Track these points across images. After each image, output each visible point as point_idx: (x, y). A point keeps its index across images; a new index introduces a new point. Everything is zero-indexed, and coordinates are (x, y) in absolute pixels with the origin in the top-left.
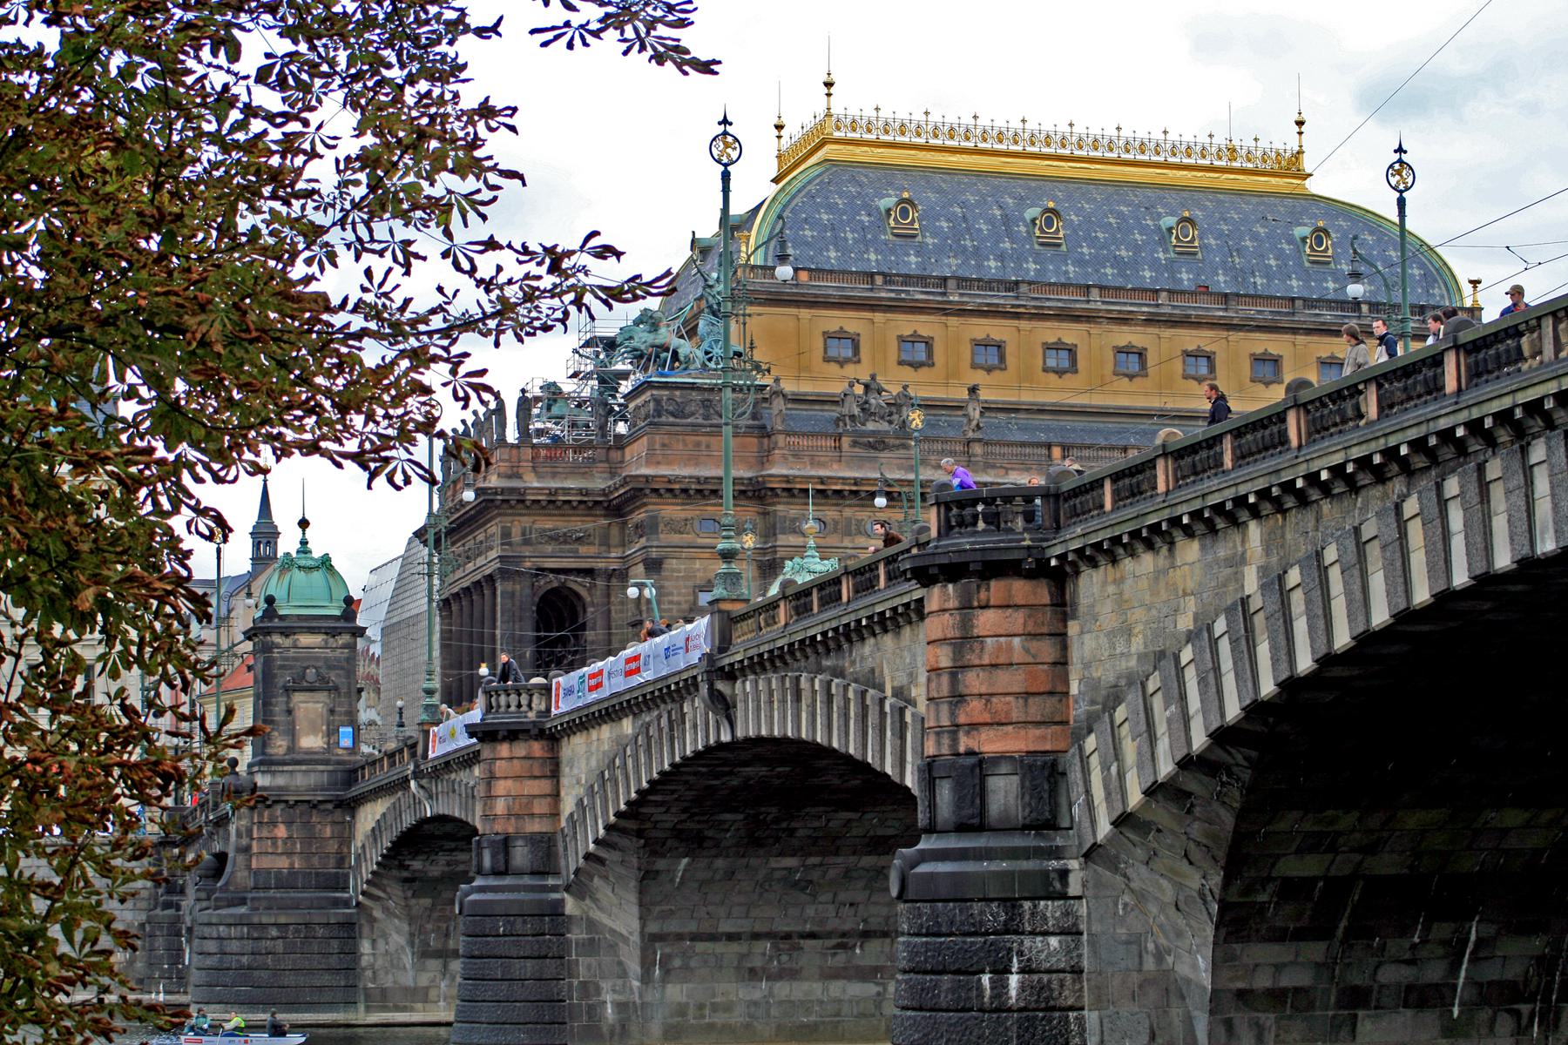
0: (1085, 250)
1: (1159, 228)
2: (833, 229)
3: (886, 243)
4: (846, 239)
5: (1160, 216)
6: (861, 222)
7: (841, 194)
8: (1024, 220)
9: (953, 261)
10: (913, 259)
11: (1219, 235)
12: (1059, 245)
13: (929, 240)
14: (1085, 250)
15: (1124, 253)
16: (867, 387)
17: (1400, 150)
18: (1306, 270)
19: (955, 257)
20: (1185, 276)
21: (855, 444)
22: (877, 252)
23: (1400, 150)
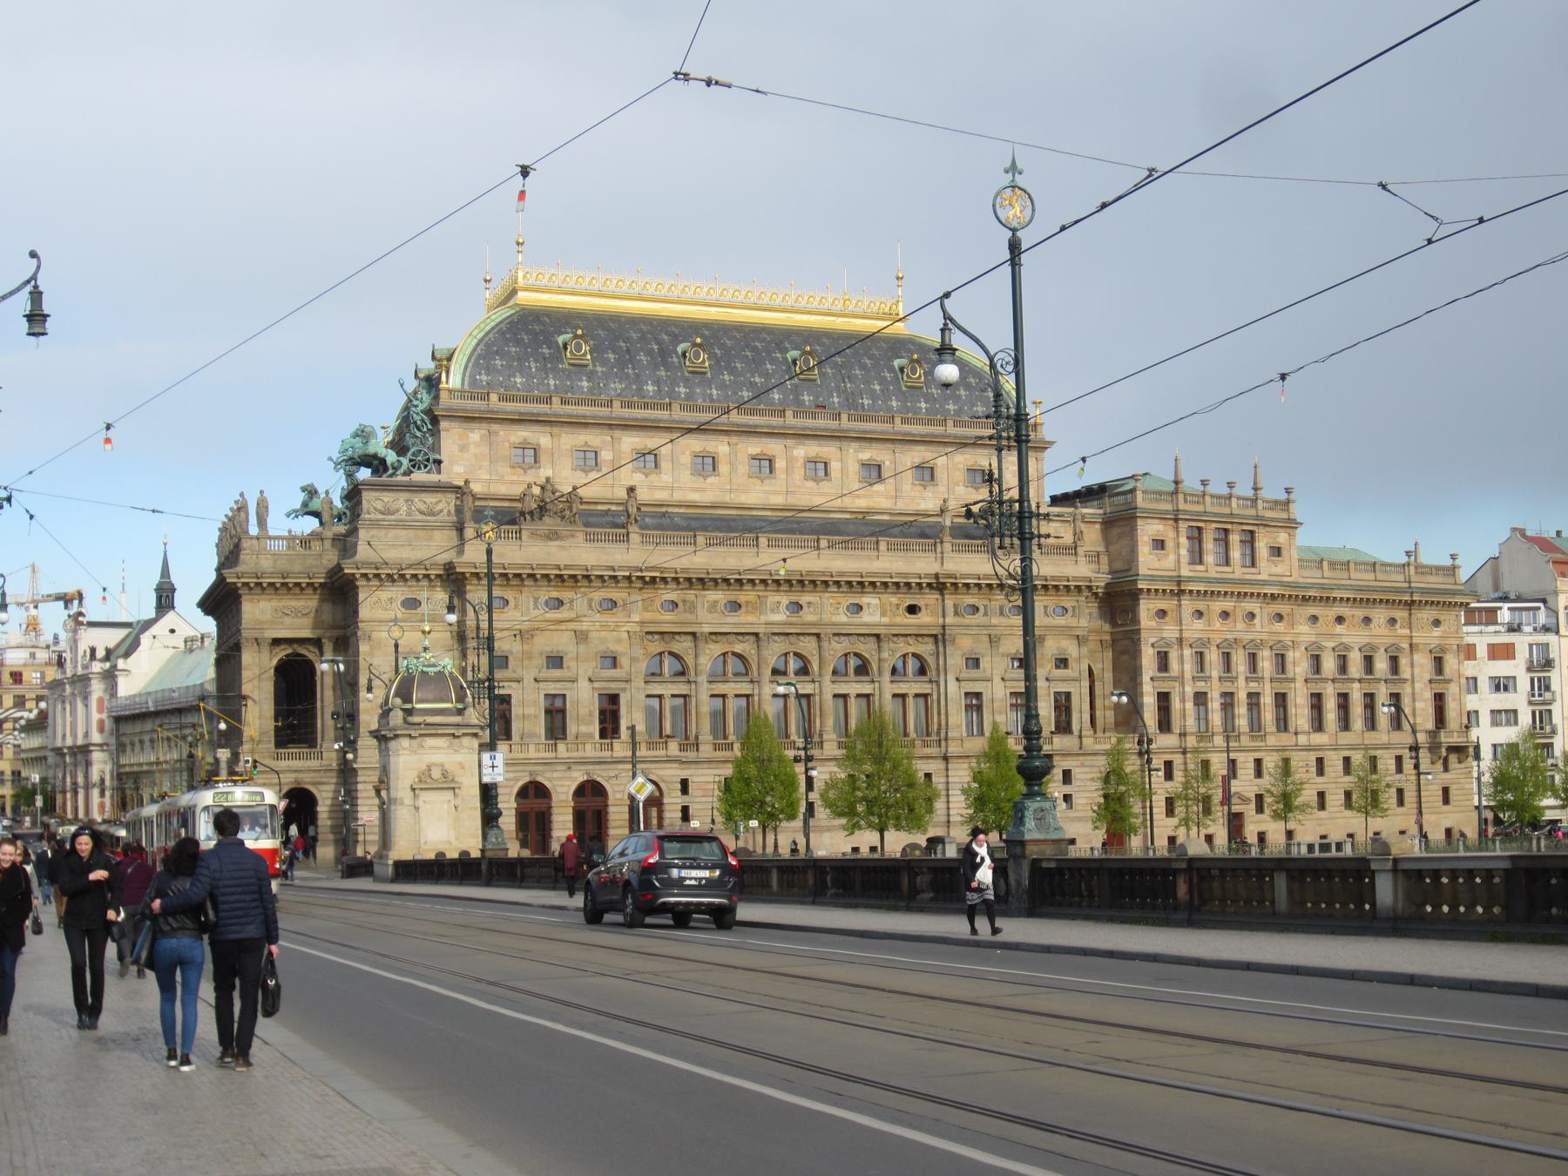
0: (726, 377)
1: (786, 359)
2: (519, 359)
3: (563, 370)
5: (787, 351)
6: (543, 354)
8: (676, 353)
10: (585, 384)
12: (705, 373)
13: (599, 369)
14: (726, 377)
15: (757, 380)
16: (543, 488)
17: (1013, 169)
18: (904, 393)
19: (620, 382)
20: (806, 398)
22: (555, 378)
23: (1013, 169)
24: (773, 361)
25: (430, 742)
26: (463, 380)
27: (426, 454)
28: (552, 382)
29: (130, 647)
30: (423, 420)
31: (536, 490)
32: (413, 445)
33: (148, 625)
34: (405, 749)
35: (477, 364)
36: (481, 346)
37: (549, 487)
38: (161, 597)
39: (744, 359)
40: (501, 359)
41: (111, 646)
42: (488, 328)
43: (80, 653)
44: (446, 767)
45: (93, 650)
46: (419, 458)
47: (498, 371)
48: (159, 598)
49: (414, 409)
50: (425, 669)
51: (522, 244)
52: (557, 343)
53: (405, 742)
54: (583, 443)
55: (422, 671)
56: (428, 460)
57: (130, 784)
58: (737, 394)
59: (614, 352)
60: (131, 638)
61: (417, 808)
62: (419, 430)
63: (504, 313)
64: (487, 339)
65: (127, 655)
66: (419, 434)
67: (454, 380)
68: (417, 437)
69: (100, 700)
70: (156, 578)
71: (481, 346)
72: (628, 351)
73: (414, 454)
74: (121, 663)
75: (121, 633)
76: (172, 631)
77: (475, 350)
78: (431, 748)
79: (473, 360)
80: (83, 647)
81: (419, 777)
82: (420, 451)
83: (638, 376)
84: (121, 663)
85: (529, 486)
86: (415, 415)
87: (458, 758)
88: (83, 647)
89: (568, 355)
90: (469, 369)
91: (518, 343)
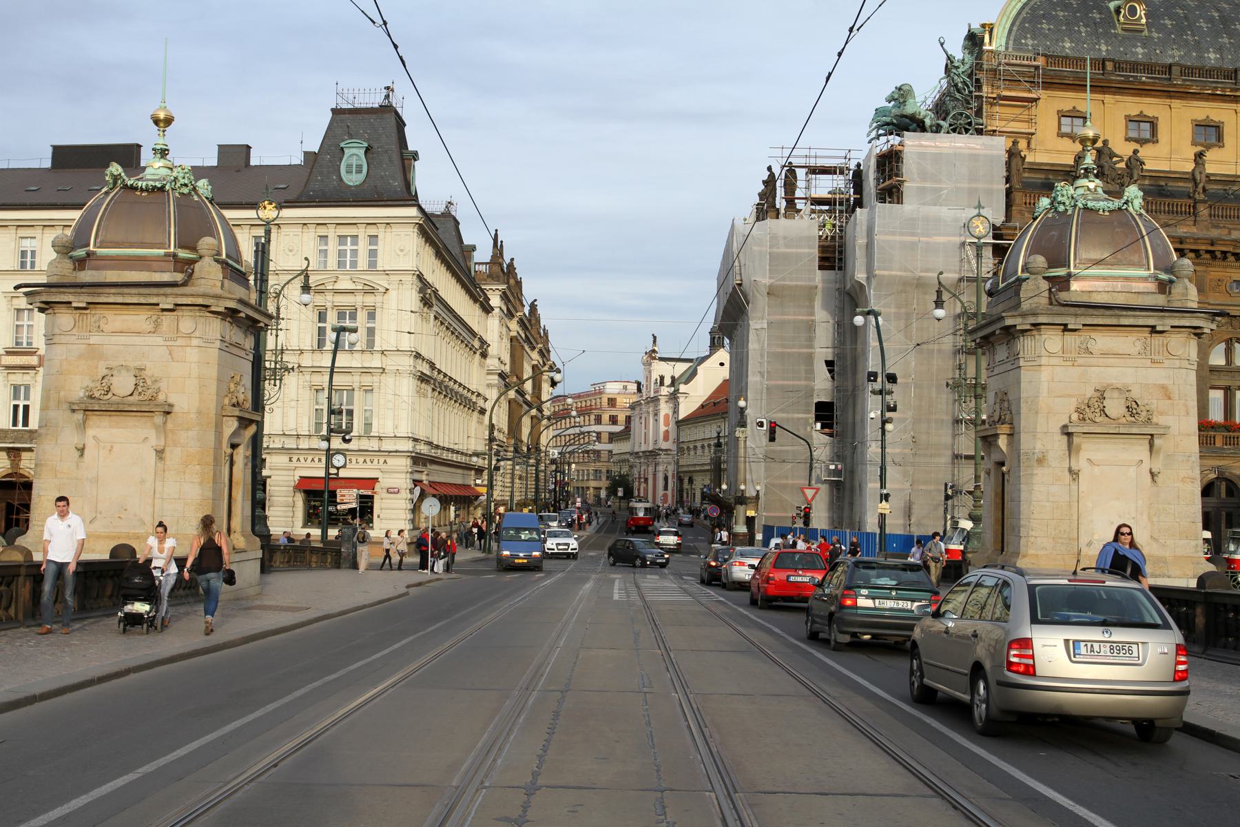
2: (1068, 24)
3: (1116, 35)
4: (1081, 33)
6: (1094, 18)
9: (1176, 53)
10: (1140, 50)
22: (1106, 44)
25: (1103, 341)
26: (1007, 43)
27: (968, 117)
28: (1104, 48)
29: (691, 375)
30: (964, 83)
32: (954, 108)
33: (703, 360)
34: (1051, 355)
35: (1022, 27)
36: (1027, 9)
37: (1106, 151)
38: (714, 338)
40: (1048, 24)
44: (1136, 393)
45: (662, 378)
46: (962, 122)
47: (1046, 36)
48: (713, 340)
49: (954, 71)
50: (1090, 204)
52: (1108, 8)
53: (1051, 341)
55: (1086, 208)
56: (970, 124)
57: (686, 481)
59: (1170, 19)
60: (691, 371)
61: (1074, 474)
62: (959, 91)
65: (686, 383)
66: (958, 96)
67: (996, 43)
68: (958, 100)
69: (667, 416)
71: (1027, 9)
72: (1186, 18)
73: (954, 117)
74: (683, 388)
77: (1019, 13)
78: (1104, 354)
79: (1018, 23)
80: (655, 376)
81: (1078, 410)
82: (961, 114)
83: (1198, 43)
84: (683, 388)
86: (956, 77)
87: (1157, 376)
89: (1122, 19)
90: (1013, 33)
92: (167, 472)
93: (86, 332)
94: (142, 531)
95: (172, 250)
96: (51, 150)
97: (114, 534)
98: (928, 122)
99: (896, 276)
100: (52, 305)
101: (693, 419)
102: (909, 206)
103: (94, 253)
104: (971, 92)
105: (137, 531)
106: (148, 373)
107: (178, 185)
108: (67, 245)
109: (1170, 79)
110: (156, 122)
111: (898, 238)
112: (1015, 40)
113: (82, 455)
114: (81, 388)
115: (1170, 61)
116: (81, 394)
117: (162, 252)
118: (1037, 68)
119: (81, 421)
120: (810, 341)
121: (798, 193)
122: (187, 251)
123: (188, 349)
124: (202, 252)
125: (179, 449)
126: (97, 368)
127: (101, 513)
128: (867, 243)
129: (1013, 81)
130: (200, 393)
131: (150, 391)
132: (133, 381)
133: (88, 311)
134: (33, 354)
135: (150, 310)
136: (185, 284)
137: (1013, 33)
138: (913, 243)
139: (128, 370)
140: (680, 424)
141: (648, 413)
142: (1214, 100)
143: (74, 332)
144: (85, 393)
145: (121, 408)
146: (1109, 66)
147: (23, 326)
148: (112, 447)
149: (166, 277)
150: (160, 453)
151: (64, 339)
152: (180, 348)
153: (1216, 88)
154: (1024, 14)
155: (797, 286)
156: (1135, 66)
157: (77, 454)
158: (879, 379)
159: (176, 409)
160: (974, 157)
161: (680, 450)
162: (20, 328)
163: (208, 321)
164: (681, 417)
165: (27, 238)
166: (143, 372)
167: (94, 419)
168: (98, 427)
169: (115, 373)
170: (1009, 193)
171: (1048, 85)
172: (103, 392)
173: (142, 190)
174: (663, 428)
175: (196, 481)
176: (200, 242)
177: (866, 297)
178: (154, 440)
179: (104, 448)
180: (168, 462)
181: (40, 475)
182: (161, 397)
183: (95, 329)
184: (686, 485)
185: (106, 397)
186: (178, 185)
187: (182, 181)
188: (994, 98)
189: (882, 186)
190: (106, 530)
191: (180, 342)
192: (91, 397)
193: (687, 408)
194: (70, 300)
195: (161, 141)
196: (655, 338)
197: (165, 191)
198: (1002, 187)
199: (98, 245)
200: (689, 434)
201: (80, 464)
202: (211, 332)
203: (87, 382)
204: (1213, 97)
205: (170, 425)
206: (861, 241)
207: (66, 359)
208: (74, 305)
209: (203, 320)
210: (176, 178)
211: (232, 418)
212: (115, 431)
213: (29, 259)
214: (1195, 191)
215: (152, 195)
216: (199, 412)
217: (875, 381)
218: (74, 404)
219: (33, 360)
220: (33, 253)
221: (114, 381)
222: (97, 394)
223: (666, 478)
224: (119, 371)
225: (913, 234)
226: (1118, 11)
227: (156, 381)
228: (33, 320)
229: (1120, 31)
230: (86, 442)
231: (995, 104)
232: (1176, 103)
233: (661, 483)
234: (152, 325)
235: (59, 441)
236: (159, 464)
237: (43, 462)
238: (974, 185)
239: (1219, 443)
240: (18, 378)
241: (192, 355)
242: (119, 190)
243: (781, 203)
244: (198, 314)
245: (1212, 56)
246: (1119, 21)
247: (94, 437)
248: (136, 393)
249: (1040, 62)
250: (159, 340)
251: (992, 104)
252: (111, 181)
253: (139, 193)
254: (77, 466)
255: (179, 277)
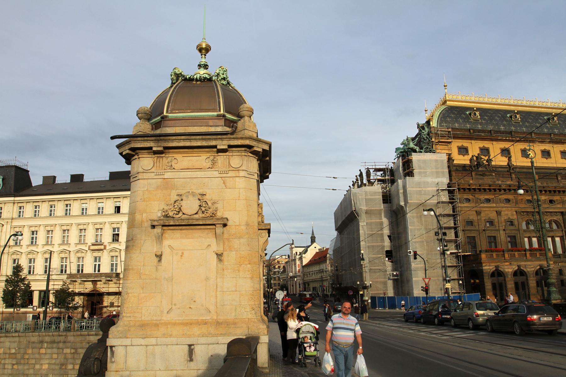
3: (471, 122)
4: (460, 121)
6: (463, 117)
7: (456, 111)
9: (491, 127)
10: (479, 126)
11: (562, 121)
21: (476, 174)
24: (541, 119)
26: (437, 125)
28: (468, 126)
29: (305, 251)
30: (427, 137)
31: (475, 158)
32: (424, 146)
35: (441, 120)
36: (441, 114)
39: (531, 119)
41: (301, 252)
42: (442, 110)
43: (293, 253)
45: (296, 253)
47: (449, 122)
48: (312, 240)
51: (446, 86)
52: (467, 114)
54: (483, 146)
57: (307, 285)
58: (532, 129)
59: (486, 117)
63: (443, 107)
64: (443, 112)
65: (305, 254)
67: (434, 124)
69: (299, 265)
70: (311, 235)
71: (441, 114)
72: (491, 116)
74: (304, 255)
75: (303, 249)
76: (315, 247)
79: (440, 119)
82: (427, 148)
84: (304, 255)
85: (473, 156)
86: (423, 136)
88: (294, 252)
89: (472, 117)
90: (439, 122)
91: (454, 114)
92: (225, 271)
93: (162, 169)
94: (208, 318)
95: (222, 112)
96: (109, 174)
97: (187, 321)
98: (417, 150)
99: (415, 203)
100: (138, 151)
101: (308, 265)
102: (417, 178)
103: (166, 117)
104: (429, 140)
105: (204, 318)
106: (206, 198)
107: (220, 78)
108: (147, 112)
109: (491, 135)
110: (200, 50)
111: (415, 189)
112: (440, 124)
113: (160, 261)
114: (159, 210)
115: (490, 129)
116: (159, 214)
117: (215, 114)
118: (449, 132)
119: (160, 234)
120: (382, 229)
121: (372, 178)
122: (231, 115)
123: (237, 179)
124: (242, 113)
125: (234, 252)
126: (170, 195)
127: (175, 305)
128: (403, 192)
129: (443, 136)
130: (247, 211)
131: (211, 210)
132: (198, 203)
133: (163, 155)
134: (102, 245)
135: (208, 152)
136: (232, 133)
137: (439, 122)
138: (420, 191)
139: (194, 196)
140: (303, 267)
141: (292, 264)
142: (506, 141)
143: (153, 170)
144: (162, 213)
145: (191, 222)
146: (472, 131)
147: (98, 235)
148: (183, 253)
149: (219, 129)
150: (219, 256)
151: (146, 176)
152: (231, 178)
153: (507, 137)
154: (441, 116)
155: (376, 210)
156: (479, 131)
157: (156, 260)
158: (440, 235)
159: (229, 223)
160: (436, 161)
161: (304, 275)
162: (97, 236)
163: (250, 159)
164: (304, 265)
165: (100, 203)
166: (204, 197)
167: (169, 233)
168: (172, 238)
169: (184, 198)
170: (450, 172)
171: (455, 138)
172: (175, 212)
173: (197, 80)
174: (298, 269)
175: (248, 276)
176: (241, 107)
177: (405, 211)
178: (215, 247)
179: (177, 254)
180: (226, 263)
181: (127, 277)
182: (219, 214)
183: (169, 168)
184: (307, 286)
185: (178, 216)
186: (220, 78)
187: (222, 76)
188: (437, 142)
189: (405, 172)
190: (180, 318)
191: (231, 174)
192: (167, 216)
193: (305, 262)
194: (151, 146)
195: (203, 60)
196: (293, 240)
197: (212, 81)
198: (447, 170)
199: (169, 112)
200: (306, 269)
201: (159, 267)
202: (252, 167)
203: (163, 206)
204: (506, 140)
205: (226, 236)
206: (401, 191)
207: (147, 190)
208: (154, 149)
209: (246, 158)
210: (218, 74)
211: (264, 231)
212: (185, 241)
213: (101, 210)
214: (510, 170)
215: (203, 83)
216: (247, 225)
217: (438, 235)
218: (154, 221)
219: (102, 247)
220: (103, 208)
221: (183, 203)
222: (171, 214)
223: (300, 284)
224: (187, 196)
225: (420, 188)
226: (470, 114)
227: (214, 203)
228: (102, 232)
229: (472, 121)
230: (163, 250)
231: (437, 145)
232: (494, 143)
233: (298, 286)
234: (210, 163)
235: (142, 251)
236: (219, 265)
237: (130, 267)
238: (437, 170)
239: (538, 256)
240: (96, 254)
241: (241, 183)
242: (181, 81)
243: (365, 181)
244: (243, 154)
245: (502, 128)
246: (471, 117)
247: (170, 246)
248: (200, 212)
249: (450, 130)
250: (216, 174)
251: (436, 145)
252: (175, 78)
253: (195, 82)
254: (157, 269)
255: (228, 129)
